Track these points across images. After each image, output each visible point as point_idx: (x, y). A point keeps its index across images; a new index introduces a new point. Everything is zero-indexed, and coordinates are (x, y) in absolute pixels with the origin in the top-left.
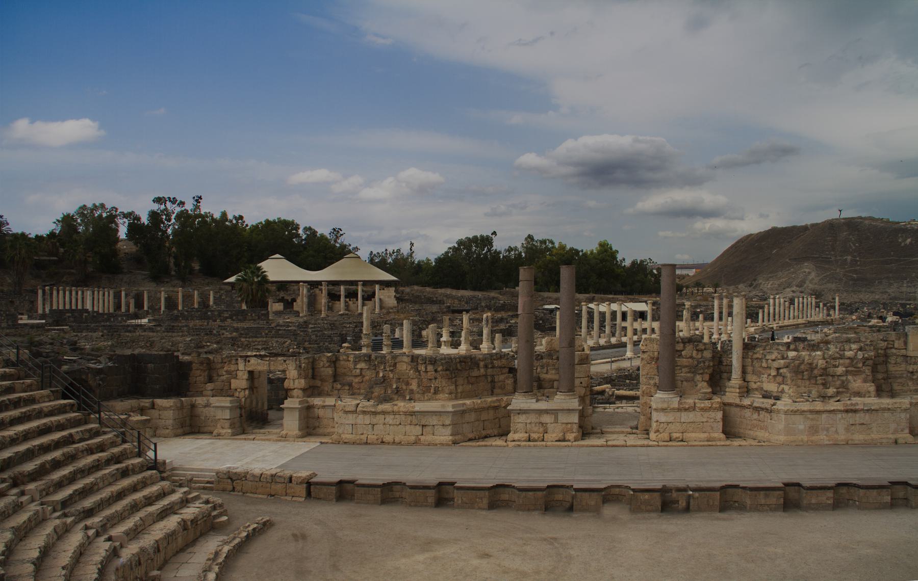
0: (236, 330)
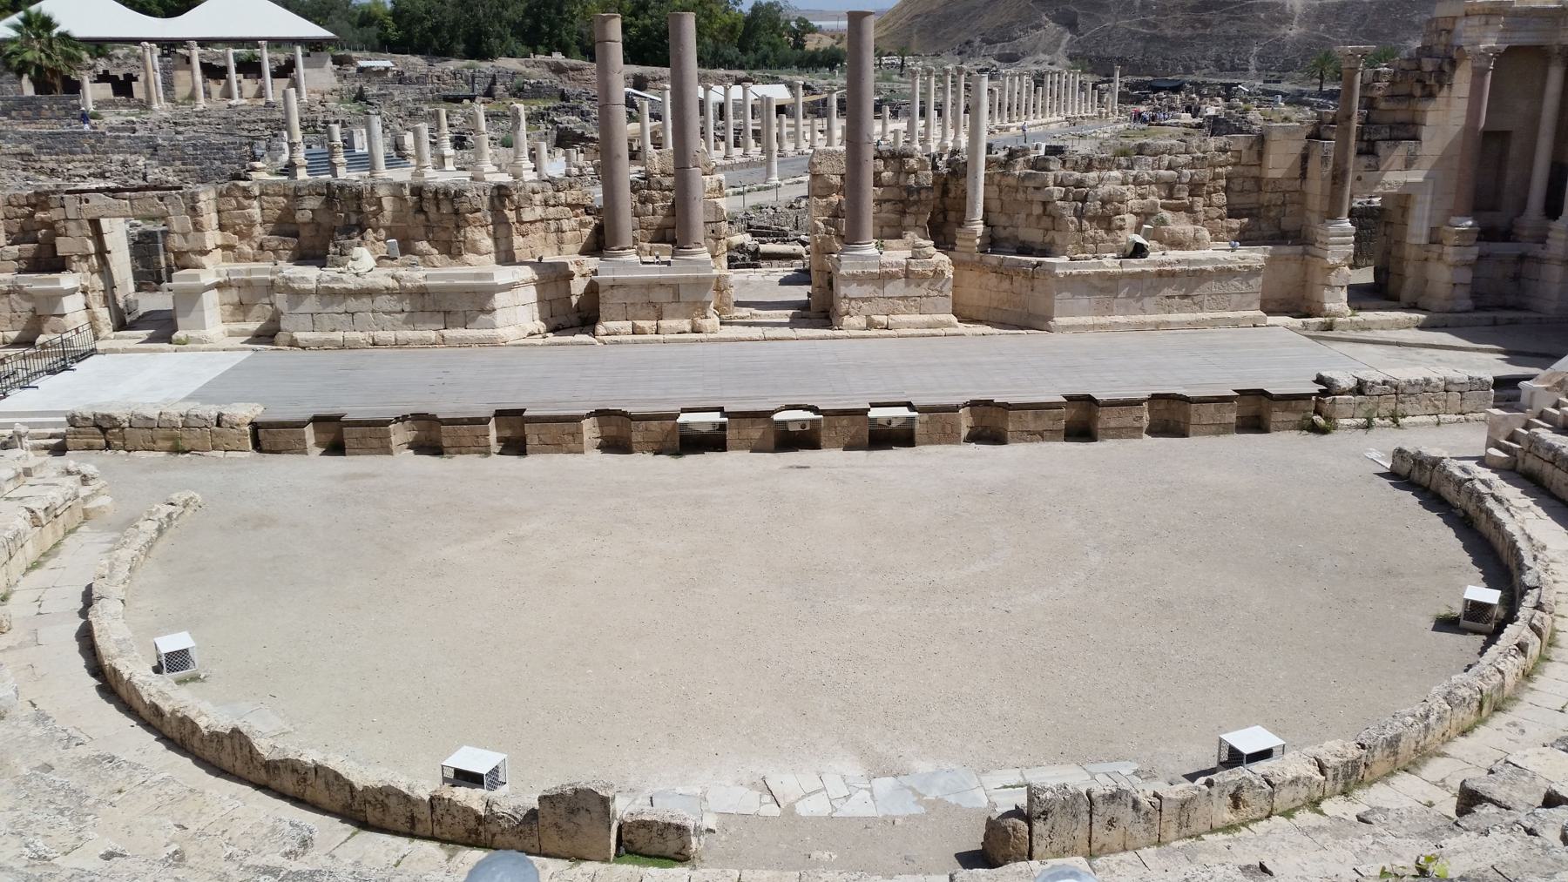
0: (27, 138)
